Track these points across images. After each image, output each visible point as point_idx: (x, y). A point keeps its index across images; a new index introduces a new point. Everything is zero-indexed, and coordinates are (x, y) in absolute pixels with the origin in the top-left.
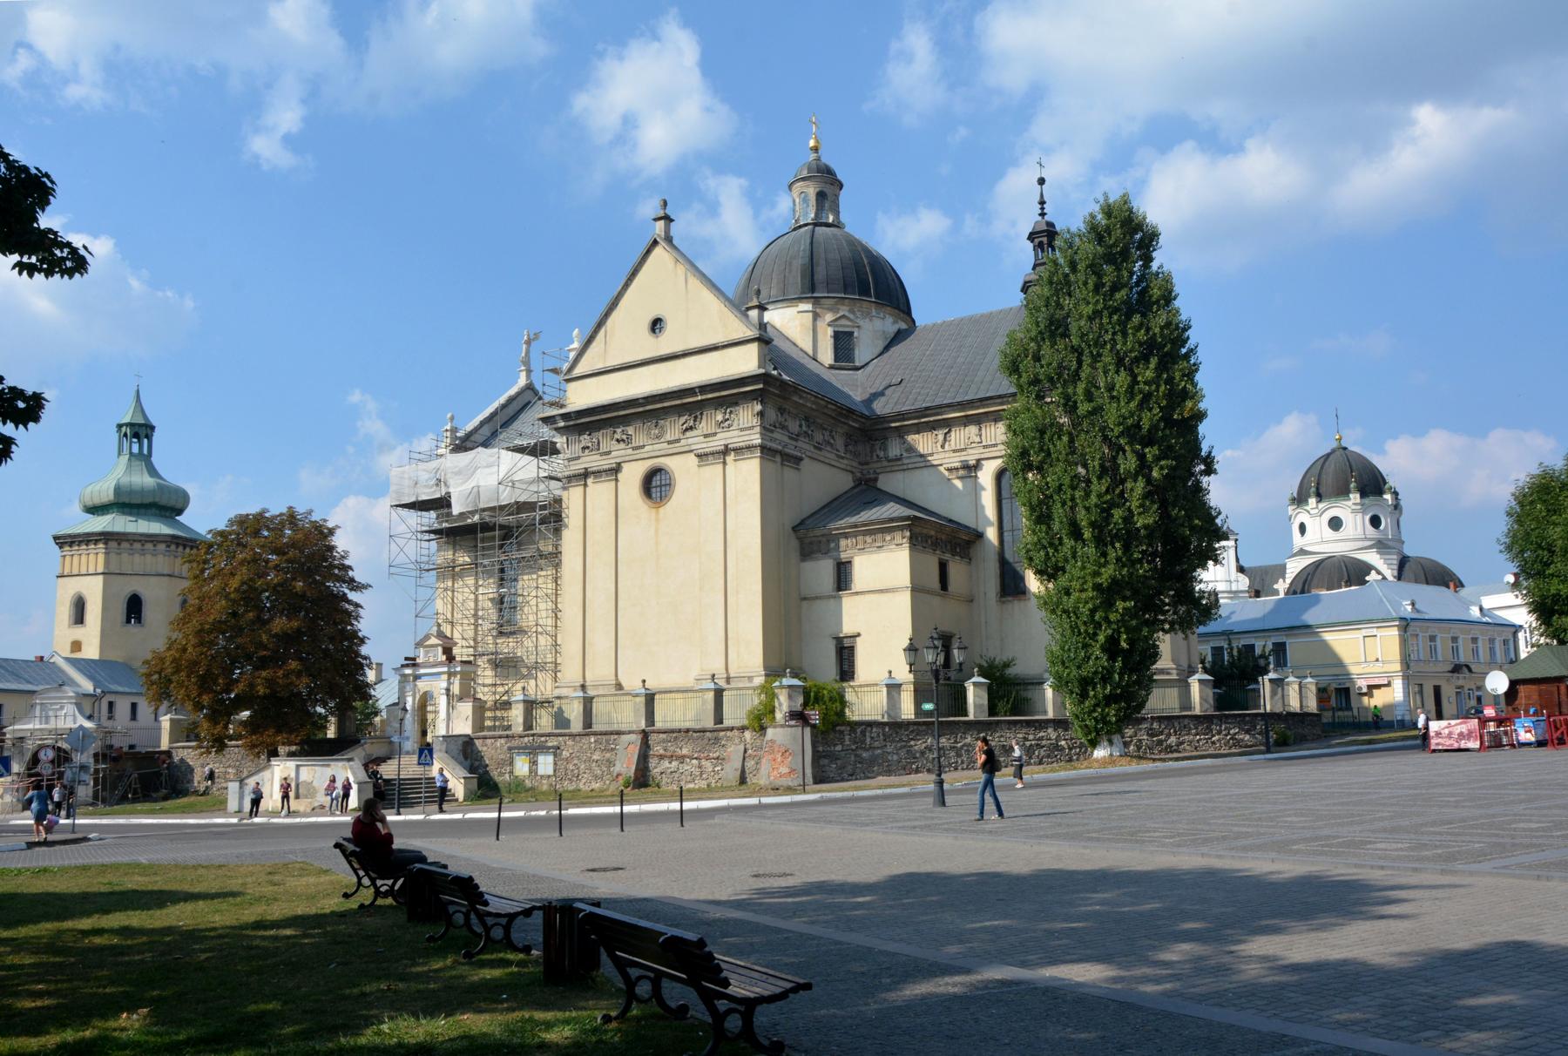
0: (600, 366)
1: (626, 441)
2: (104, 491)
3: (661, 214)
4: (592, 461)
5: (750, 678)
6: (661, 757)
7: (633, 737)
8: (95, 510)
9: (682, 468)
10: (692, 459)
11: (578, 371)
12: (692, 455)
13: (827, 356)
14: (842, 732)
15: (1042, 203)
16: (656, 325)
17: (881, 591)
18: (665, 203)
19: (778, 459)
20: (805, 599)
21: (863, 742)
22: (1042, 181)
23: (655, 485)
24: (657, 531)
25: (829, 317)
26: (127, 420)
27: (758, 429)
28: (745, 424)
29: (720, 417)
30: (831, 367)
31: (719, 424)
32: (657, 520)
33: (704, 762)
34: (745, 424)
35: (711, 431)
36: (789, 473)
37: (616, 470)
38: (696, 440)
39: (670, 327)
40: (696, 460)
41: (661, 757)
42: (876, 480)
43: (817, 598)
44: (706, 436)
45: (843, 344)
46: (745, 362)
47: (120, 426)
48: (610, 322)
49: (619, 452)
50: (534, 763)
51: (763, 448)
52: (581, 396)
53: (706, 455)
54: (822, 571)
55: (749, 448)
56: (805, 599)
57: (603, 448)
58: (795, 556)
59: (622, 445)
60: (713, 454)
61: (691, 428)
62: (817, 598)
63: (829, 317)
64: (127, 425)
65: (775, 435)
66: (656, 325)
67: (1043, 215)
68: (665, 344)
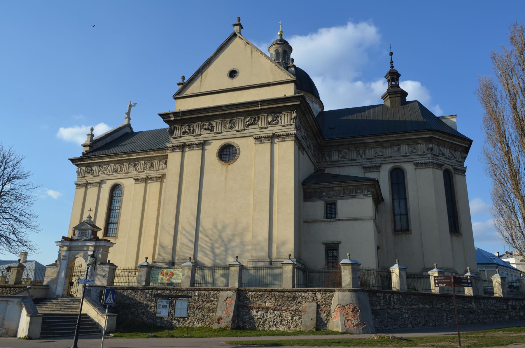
0: (197, 91)
1: (211, 129)
3: (237, 23)
7: (230, 293)
12: (252, 138)
14: (379, 297)
15: (392, 62)
16: (233, 74)
17: (355, 220)
18: (239, 19)
20: (305, 222)
21: (390, 304)
22: (391, 54)
23: (227, 153)
24: (226, 178)
27: (294, 126)
28: (287, 123)
29: (270, 119)
32: (227, 172)
33: (284, 313)
35: (264, 126)
37: (203, 145)
38: (254, 130)
42: (324, 170)
43: (314, 222)
44: (260, 128)
49: (206, 135)
50: (173, 306)
53: (260, 138)
54: (318, 208)
55: (288, 135)
56: (305, 222)
57: (197, 132)
58: (302, 197)
59: (208, 132)
60: (265, 137)
62: (314, 222)
66: (233, 74)
68: (236, 83)
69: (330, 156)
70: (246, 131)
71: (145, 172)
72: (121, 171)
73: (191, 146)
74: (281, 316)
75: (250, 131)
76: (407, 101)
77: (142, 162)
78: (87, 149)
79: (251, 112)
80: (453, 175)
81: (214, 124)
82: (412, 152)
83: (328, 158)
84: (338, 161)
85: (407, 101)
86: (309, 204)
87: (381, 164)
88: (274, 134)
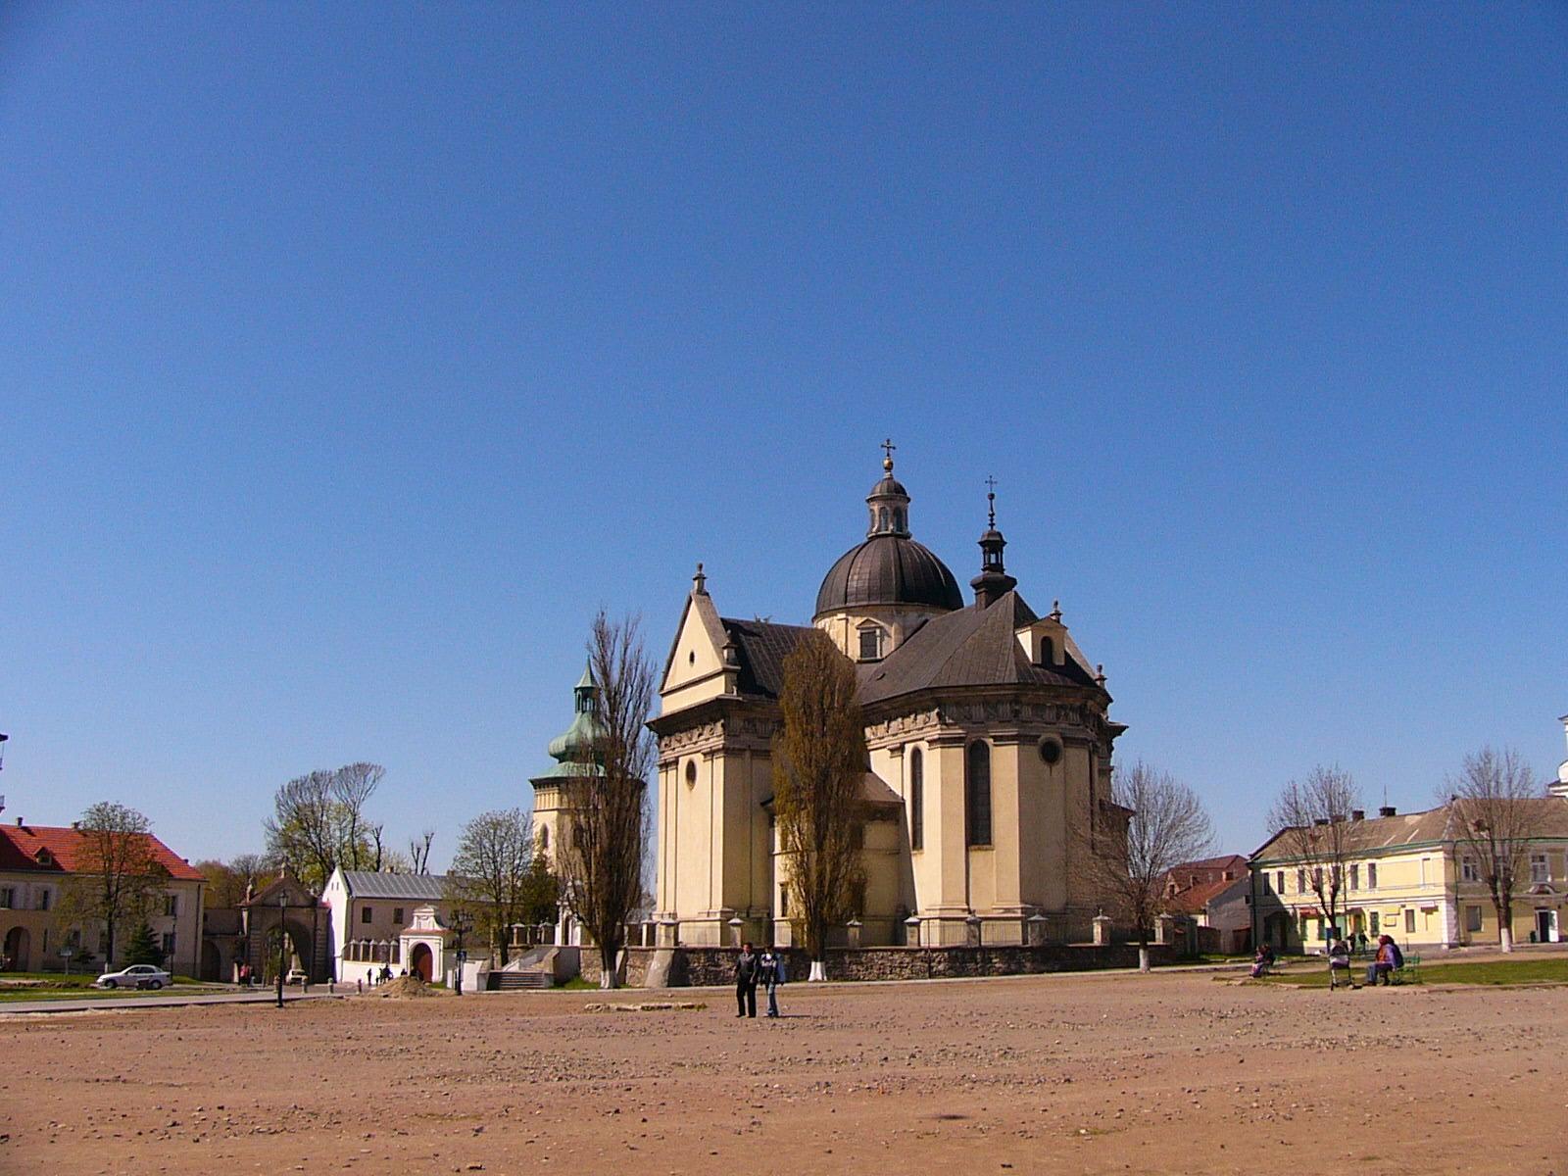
2: (559, 744)
4: (669, 755)
8: (561, 757)
10: (700, 755)
11: (667, 687)
13: (854, 651)
15: (992, 515)
19: (748, 754)
22: (992, 497)
25: (858, 621)
26: (578, 686)
30: (859, 662)
34: (714, 737)
36: (760, 764)
37: (676, 762)
45: (868, 640)
46: (716, 689)
47: (576, 690)
52: (671, 705)
61: (700, 735)
63: (858, 621)
64: (580, 688)
65: (742, 738)
67: (992, 525)
80: (991, 747)
87: (905, 743)
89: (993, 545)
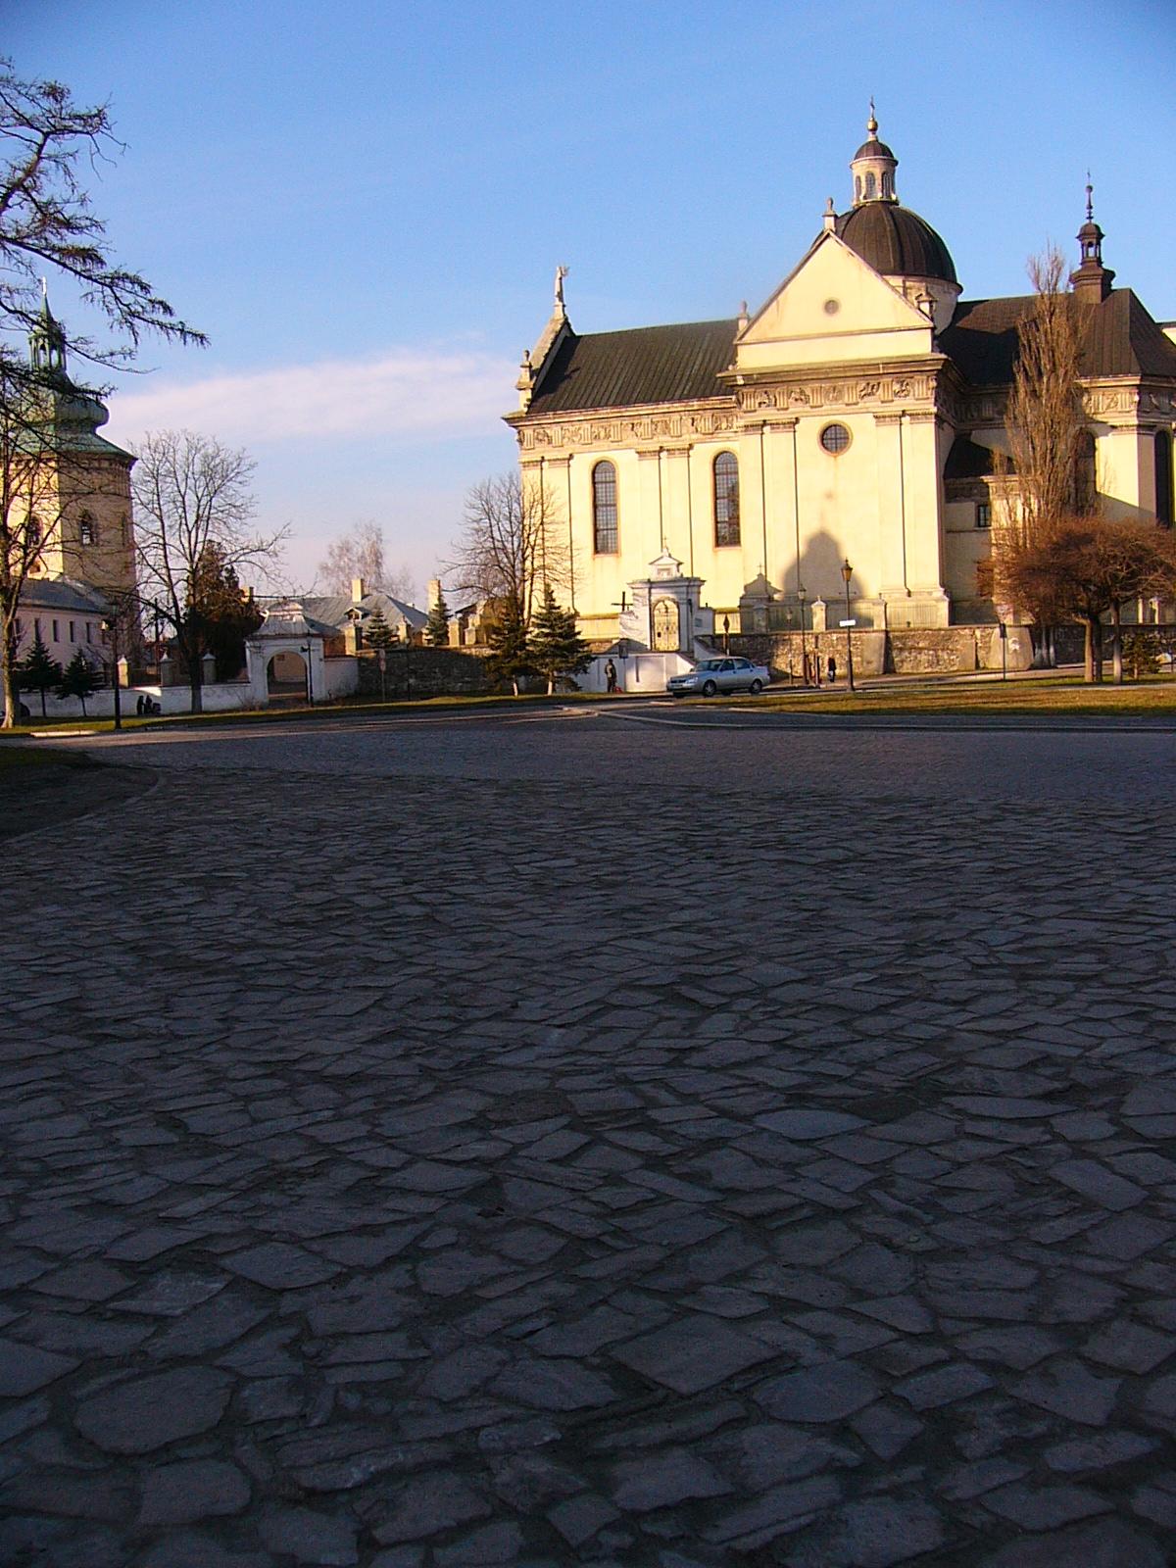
1: (803, 398)
5: (930, 593)
6: (901, 649)
9: (860, 425)
15: (1090, 207)
16: (831, 307)
22: (1090, 189)
23: (834, 439)
31: (896, 394)
33: (940, 653)
38: (873, 404)
39: (845, 308)
40: (874, 420)
41: (901, 649)
42: (970, 434)
48: (780, 297)
51: (937, 416)
56: (948, 532)
57: (781, 403)
59: (799, 403)
61: (869, 395)
66: (831, 307)
68: (838, 323)
69: (979, 410)
70: (860, 405)
71: (655, 439)
72: (608, 436)
73: (774, 425)
74: (937, 656)
75: (867, 405)
76: (1113, 288)
77: (646, 420)
78: (529, 394)
79: (869, 376)
81: (808, 392)
82: (1108, 407)
83: (975, 414)
84: (991, 420)
85: (1113, 288)
86: (953, 505)
88: (903, 411)
89: (1092, 236)
